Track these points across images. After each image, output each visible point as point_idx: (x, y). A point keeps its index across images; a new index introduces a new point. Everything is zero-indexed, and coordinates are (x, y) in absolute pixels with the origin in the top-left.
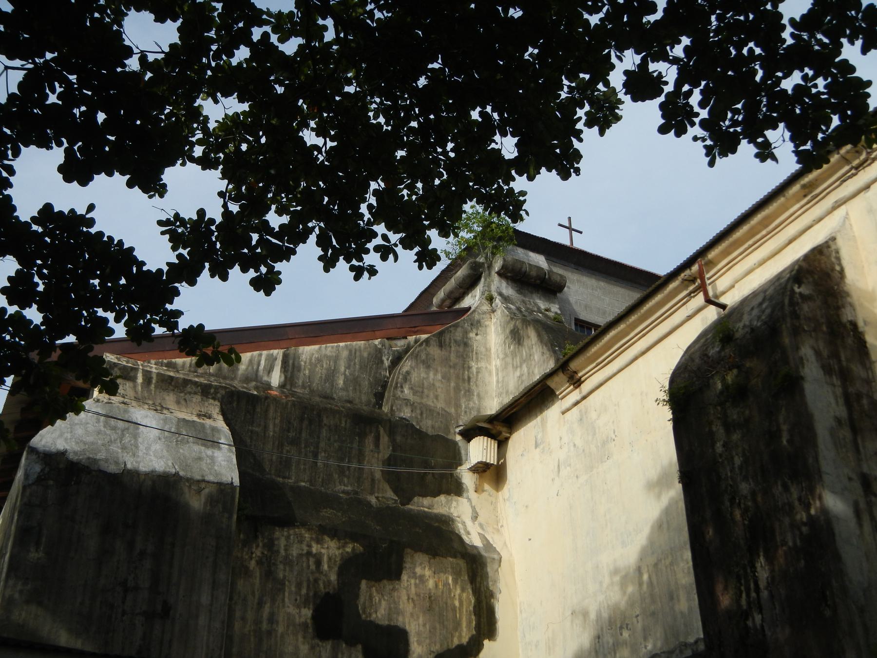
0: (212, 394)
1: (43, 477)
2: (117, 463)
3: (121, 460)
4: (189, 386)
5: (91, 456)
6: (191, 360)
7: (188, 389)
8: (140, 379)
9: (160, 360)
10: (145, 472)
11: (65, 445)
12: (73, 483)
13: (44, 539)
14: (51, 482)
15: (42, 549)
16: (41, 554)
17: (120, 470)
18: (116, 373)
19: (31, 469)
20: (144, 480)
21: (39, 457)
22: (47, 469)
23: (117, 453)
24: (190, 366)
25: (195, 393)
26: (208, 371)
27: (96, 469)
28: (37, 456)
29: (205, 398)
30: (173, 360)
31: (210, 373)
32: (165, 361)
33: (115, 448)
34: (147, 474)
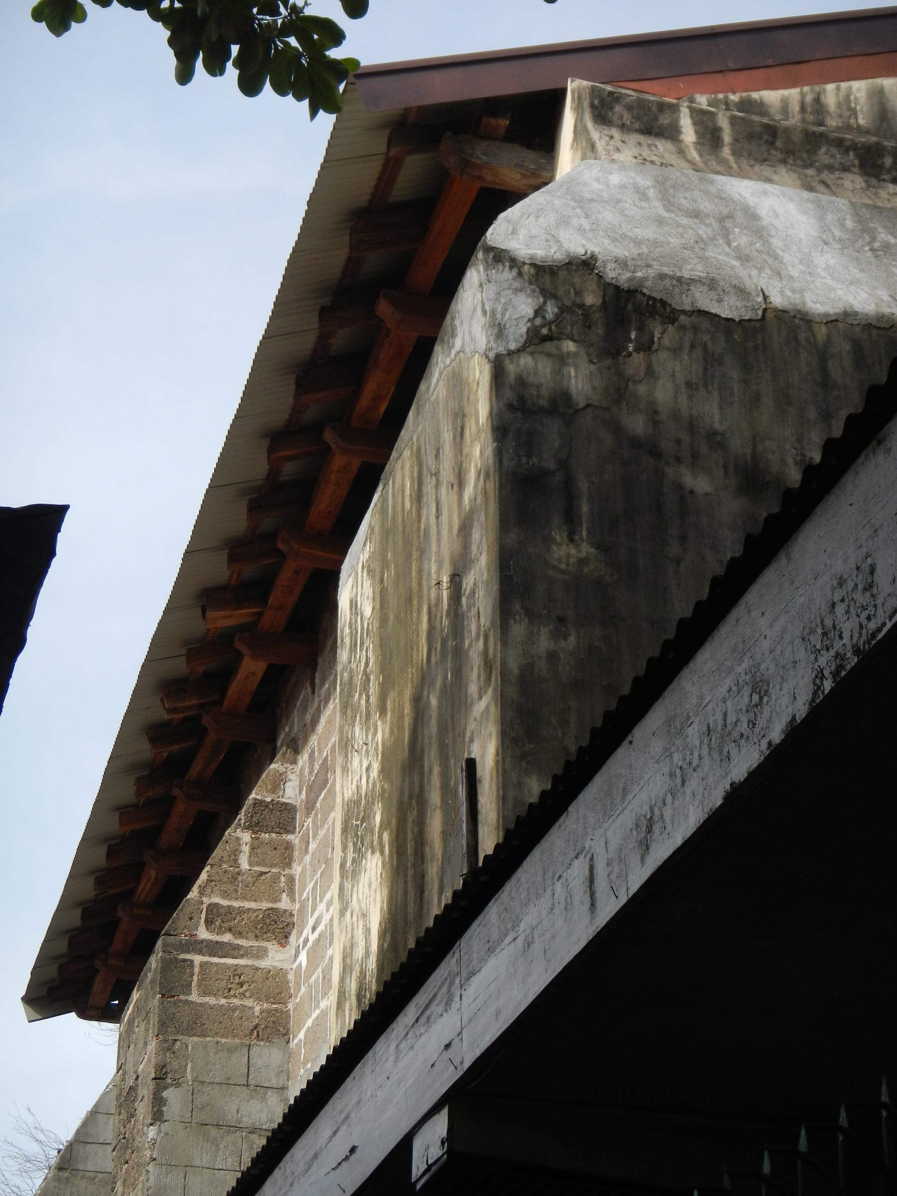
0: (889, 171)
1: (545, 331)
2: (741, 292)
3: (749, 285)
4: (823, 150)
5: (666, 270)
6: (803, 95)
7: (823, 155)
8: (689, 134)
9: (721, 96)
10: (826, 315)
11: (584, 242)
12: (631, 347)
13: (585, 508)
14: (570, 346)
15: (584, 533)
16: (586, 549)
17: (754, 309)
18: (621, 117)
19: (505, 310)
20: (829, 337)
21: (520, 274)
22: (551, 310)
23: (733, 268)
24: (803, 109)
25: (845, 169)
26: (852, 121)
27: (688, 308)
28: (515, 271)
29: (874, 181)
30: (755, 95)
31: (859, 126)
32: (734, 98)
33: (719, 254)
34: (832, 322)
